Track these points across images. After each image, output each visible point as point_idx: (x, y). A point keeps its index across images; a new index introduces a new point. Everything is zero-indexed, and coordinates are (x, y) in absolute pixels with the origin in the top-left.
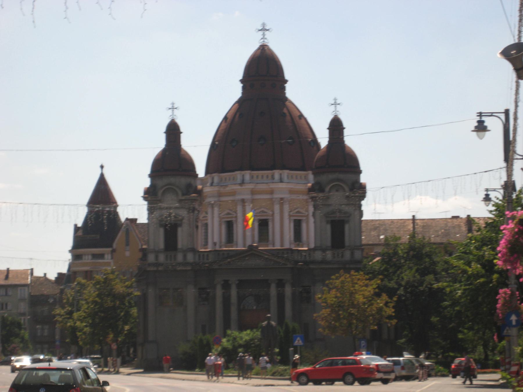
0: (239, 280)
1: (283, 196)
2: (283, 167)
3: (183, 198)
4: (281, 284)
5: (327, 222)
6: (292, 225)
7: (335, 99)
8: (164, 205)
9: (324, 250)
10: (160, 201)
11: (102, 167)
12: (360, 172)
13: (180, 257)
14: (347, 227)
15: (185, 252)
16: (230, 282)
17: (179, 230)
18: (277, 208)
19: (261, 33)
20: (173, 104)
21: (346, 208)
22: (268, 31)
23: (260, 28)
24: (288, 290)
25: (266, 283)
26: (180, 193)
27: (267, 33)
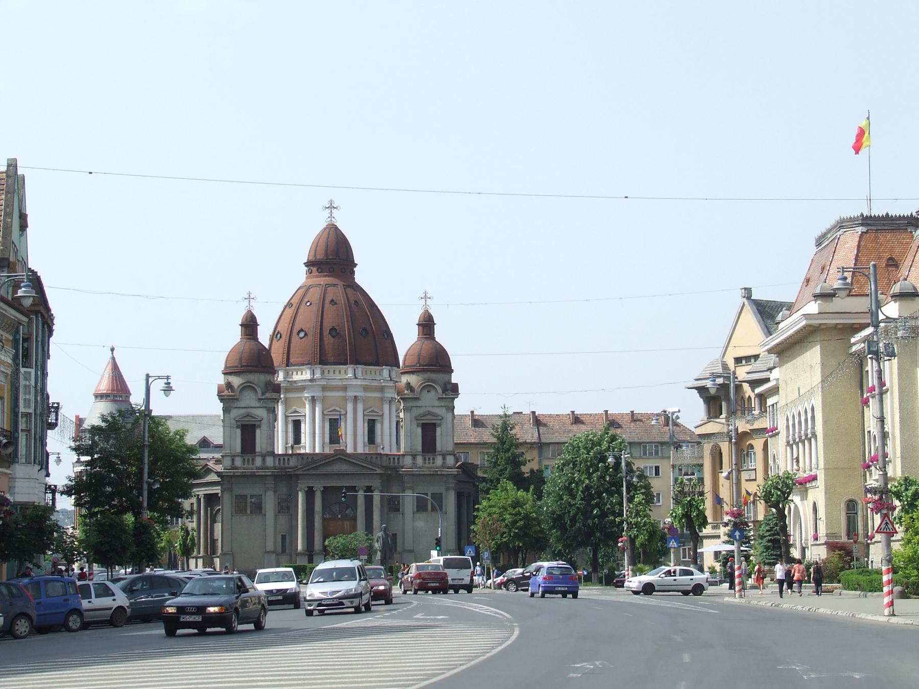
0: (323, 487)
4: (369, 489)
5: (418, 425)
6: (366, 425)
11: (112, 350)
12: (452, 371)
13: (258, 462)
14: (438, 430)
16: (314, 489)
17: (258, 432)
18: (350, 407)
19: (328, 211)
20: (249, 293)
21: (437, 411)
22: (335, 209)
23: (327, 207)
24: (377, 496)
25: (353, 489)
27: (334, 211)
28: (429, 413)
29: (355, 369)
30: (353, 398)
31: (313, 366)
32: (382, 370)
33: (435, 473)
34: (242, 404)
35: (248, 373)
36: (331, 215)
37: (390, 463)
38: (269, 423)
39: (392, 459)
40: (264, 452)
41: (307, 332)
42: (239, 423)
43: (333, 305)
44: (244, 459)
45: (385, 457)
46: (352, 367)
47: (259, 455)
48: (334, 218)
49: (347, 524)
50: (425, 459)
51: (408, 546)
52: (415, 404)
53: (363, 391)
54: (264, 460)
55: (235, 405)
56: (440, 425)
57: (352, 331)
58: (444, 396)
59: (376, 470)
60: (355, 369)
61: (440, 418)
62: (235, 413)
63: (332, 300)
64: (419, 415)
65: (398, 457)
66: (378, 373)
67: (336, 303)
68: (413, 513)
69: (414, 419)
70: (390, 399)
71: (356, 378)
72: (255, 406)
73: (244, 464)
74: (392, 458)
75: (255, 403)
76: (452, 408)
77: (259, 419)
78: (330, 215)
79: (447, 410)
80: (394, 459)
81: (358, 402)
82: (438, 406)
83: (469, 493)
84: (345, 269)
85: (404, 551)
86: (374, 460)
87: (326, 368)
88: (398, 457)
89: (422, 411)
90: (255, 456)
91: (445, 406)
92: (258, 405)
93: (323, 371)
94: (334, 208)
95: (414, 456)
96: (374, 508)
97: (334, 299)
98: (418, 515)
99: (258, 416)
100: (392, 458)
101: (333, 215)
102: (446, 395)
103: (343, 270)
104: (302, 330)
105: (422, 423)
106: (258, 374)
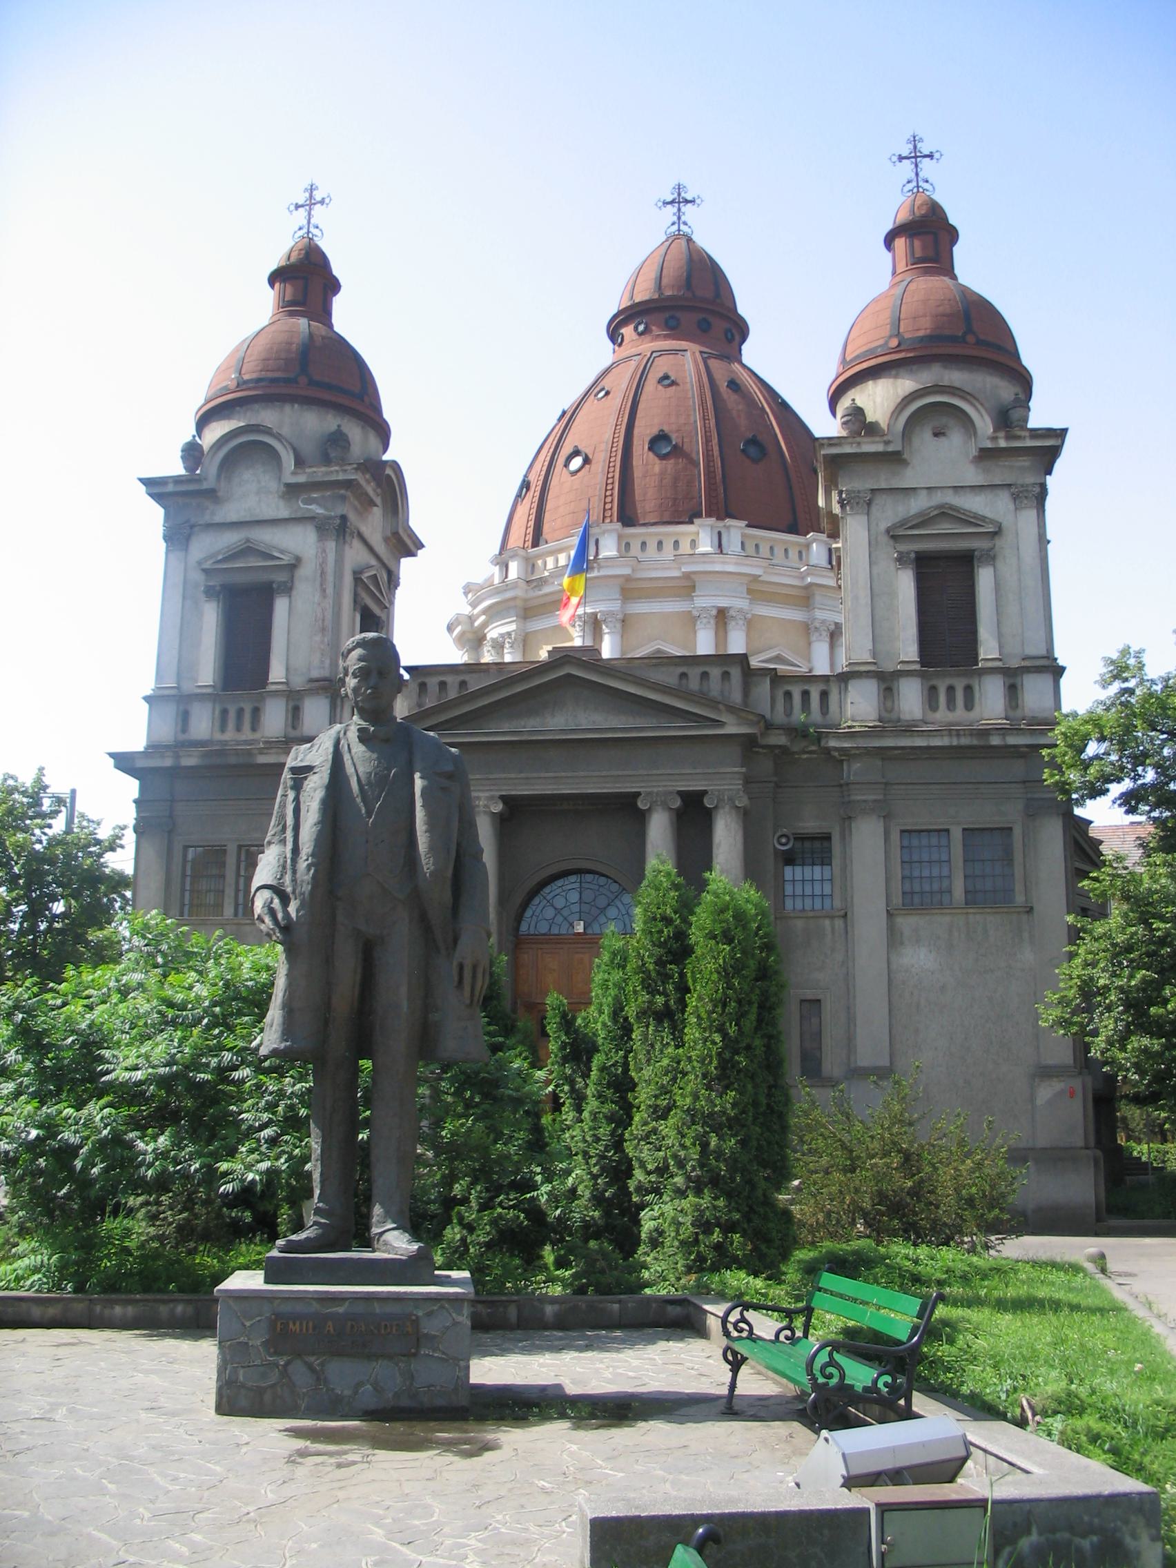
0: (502, 798)
1: (723, 603)
3: (301, 479)
5: (901, 560)
7: (914, 140)
8: (231, 511)
9: (887, 681)
10: (211, 495)
14: (984, 578)
17: (281, 606)
19: (672, 209)
21: (975, 504)
22: (689, 205)
23: (669, 199)
26: (288, 461)
27: (687, 209)
28: (946, 513)
29: (720, 534)
30: (714, 612)
32: (808, 546)
33: (975, 742)
34: (231, 511)
35: (256, 406)
36: (679, 218)
37: (789, 712)
38: (323, 573)
40: (298, 682)
41: (590, 457)
42: (215, 582)
43: (640, 334)
44: (224, 712)
45: (767, 683)
46: (712, 527)
47: (276, 693)
48: (685, 223)
50: (932, 692)
51: (869, 1053)
52: (883, 480)
53: (745, 595)
55: (207, 518)
56: (990, 557)
57: (715, 441)
58: (1003, 443)
60: (720, 534)
63: (666, 377)
64: (902, 524)
65: (822, 687)
66: (793, 554)
67: (674, 383)
68: (890, 914)
69: (884, 539)
70: (832, 627)
71: (721, 552)
73: (223, 729)
75: (276, 508)
76: (1037, 489)
77: (286, 559)
78: (675, 218)
79: (1016, 498)
80: (806, 694)
82: (981, 487)
85: (857, 1073)
86: (715, 686)
87: (634, 536)
88: (822, 687)
89: (918, 504)
90: (262, 698)
91: (1010, 485)
92: (284, 513)
93: (628, 545)
94: (687, 201)
95: (887, 681)
97: (670, 374)
98: (906, 923)
99: (282, 552)
101: (683, 218)
106: (296, 406)
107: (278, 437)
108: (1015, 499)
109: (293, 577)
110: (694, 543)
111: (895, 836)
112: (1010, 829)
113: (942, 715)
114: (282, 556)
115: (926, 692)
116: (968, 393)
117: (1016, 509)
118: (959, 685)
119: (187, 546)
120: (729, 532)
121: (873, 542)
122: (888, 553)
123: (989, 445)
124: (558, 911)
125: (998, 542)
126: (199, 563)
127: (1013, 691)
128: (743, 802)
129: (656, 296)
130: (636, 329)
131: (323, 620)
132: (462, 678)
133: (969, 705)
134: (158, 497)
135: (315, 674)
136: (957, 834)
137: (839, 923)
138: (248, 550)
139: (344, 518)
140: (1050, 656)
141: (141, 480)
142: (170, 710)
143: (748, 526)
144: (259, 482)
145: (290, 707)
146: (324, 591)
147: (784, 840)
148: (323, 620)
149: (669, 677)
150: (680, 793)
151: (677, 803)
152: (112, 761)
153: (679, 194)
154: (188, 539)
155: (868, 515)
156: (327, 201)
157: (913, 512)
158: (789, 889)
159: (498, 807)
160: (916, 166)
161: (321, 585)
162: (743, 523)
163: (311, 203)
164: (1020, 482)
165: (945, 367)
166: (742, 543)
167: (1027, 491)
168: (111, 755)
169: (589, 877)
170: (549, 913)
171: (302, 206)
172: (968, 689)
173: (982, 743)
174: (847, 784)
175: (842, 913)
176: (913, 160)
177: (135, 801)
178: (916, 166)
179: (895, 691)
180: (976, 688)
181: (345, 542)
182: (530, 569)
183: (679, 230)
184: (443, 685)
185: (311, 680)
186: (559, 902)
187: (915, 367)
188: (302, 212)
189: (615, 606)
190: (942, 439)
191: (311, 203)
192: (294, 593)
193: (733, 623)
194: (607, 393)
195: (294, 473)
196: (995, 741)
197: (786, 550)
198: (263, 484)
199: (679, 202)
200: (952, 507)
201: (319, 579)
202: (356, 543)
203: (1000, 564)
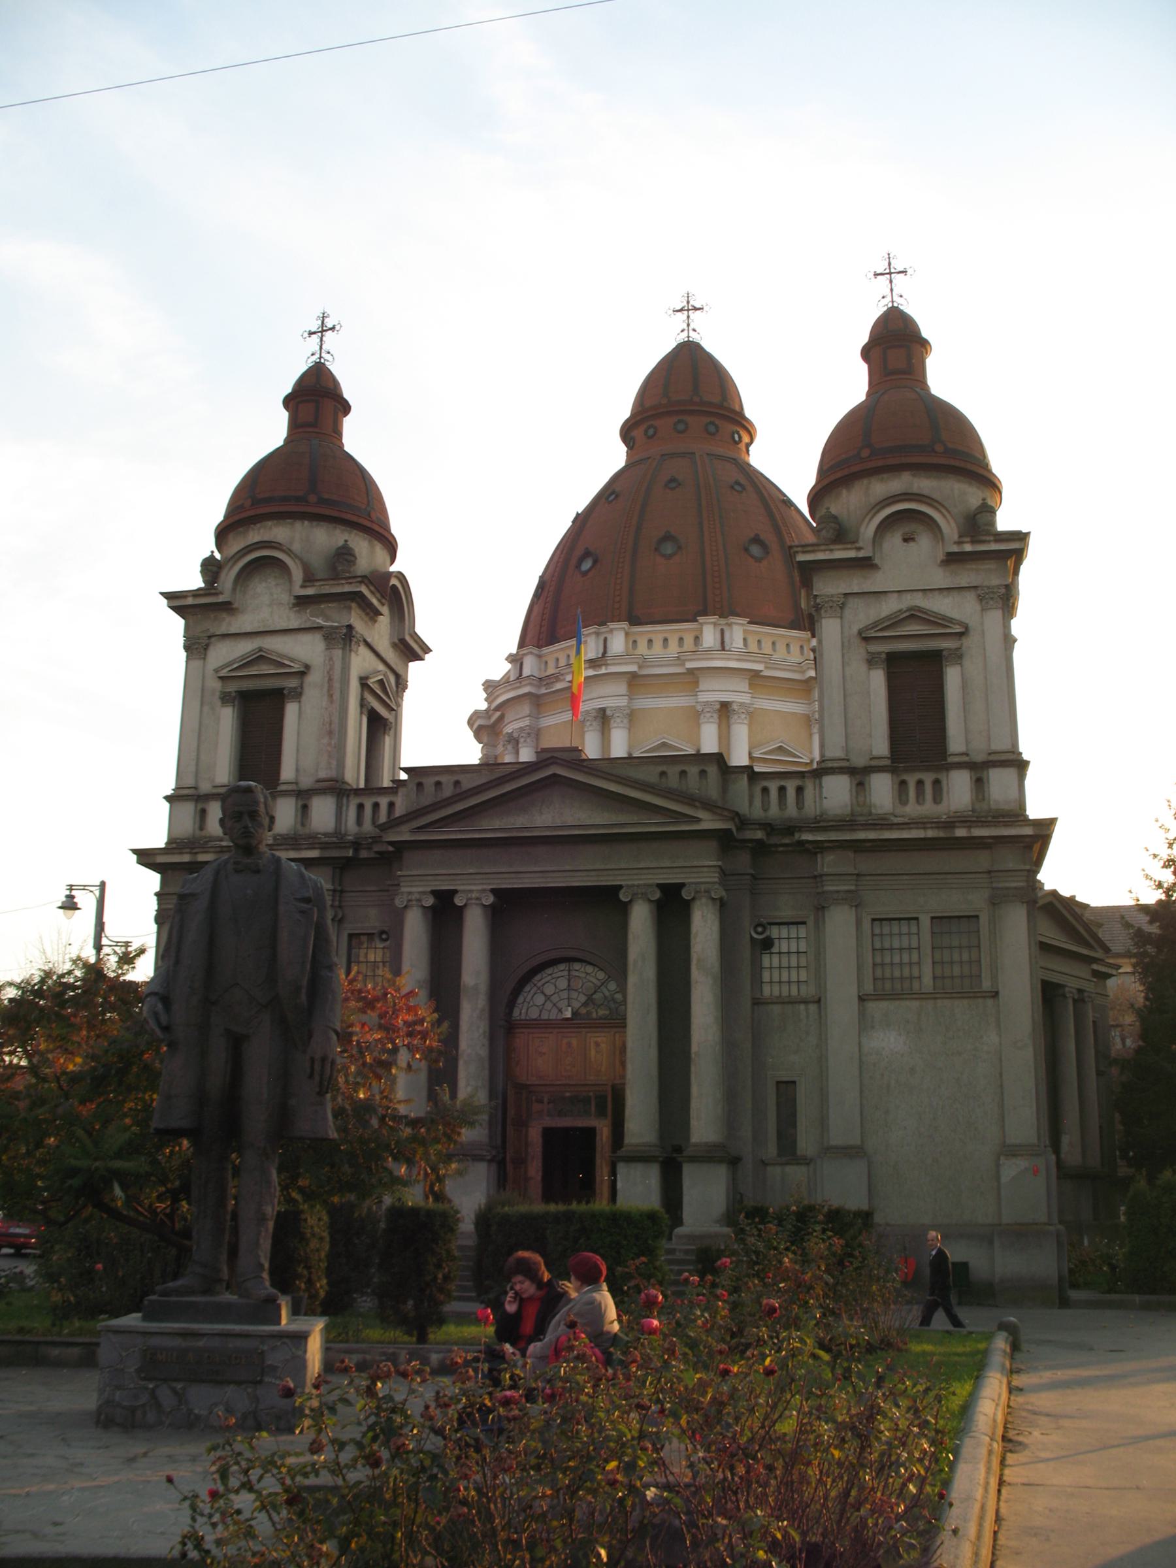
0: (493, 891)
2: (726, 610)
3: (310, 591)
5: (871, 661)
9: (859, 774)
10: (227, 607)
14: (952, 676)
15: (303, 796)
17: (291, 709)
21: (942, 605)
26: (297, 574)
28: (914, 615)
29: (722, 631)
30: (718, 706)
31: (603, 629)
33: (941, 834)
35: (270, 523)
36: (688, 325)
37: (766, 807)
38: (330, 680)
39: (774, 794)
40: (306, 782)
42: (232, 687)
45: (744, 779)
46: (715, 624)
47: (286, 793)
48: (694, 330)
49: (597, 1044)
51: (841, 1132)
52: (856, 583)
53: (747, 689)
54: (304, 810)
55: (223, 629)
56: (957, 656)
58: (968, 548)
59: (698, 820)
60: (722, 631)
61: (958, 629)
62: (223, 654)
63: (673, 480)
64: (875, 625)
65: (797, 782)
68: (862, 999)
71: (723, 649)
72: (283, 625)
74: (773, 787)
77: (297, 667)
78: (685, 326)
79: (981, 599)
80: (782, 790)
81: (732, 721)
83: (1080, 991)
84: (717, 427)
85: (830, 1151)
86: (693, 784)
89: (889, 607)
92: (295, 623)
93: (635, 642)
95: (859, 774)
96: (695, 974)
99: (292, 660)
100: (773, 787)
101: (692, 326)
102: (973, 542)
103: (712, 429)
104: (587, 554)
105: (888, 654)
106: (306, 523)
107: (289, 552)
108: (981, 600)
109: (302, 684)
110: (697, 639)
111: (866, 925)
112: (977, 917)
113: (912, 809)
114: (292, 664)
115: (896, 786)
116: (937, 502)
117: (983, 610)
118: (928, 778)
119: (205, 655)
120: (732, 630)
121: (846, 644)
122: (859, 652)
123: (955, 549)
124: (548, 998)
125: (966, 642)
126: (216, 671)
127: (979, 783)
128: (721, 893)
129: (664, 401)
130: (646, 431)
131: (330, 724)
132: (456, 778)
133: (937, 798)
134: (178, 610)
135: (322, 774)
136: (925, 921)
137: (813, 1008)
138: (261, 657)
139: (350, 627)
140: (1014, 750)
141: (162, 594)
142: (189, 808)
143: (749, 623)
144: (271, 594)
145: (299, 806)
146: (331, 696)
147: (760, 929)
148: (330, 724)
149: (650, 775)
150: (659, 886)
151: (657, 895)
152: (135, 857)
153: (688, 302)
154: (206, 647)
155: (841, 618)
156: (337, 328)
157: (883, 615)
158: (766, 976)
159: (489, 900)
160: (891, 282)
161: (328, 691)
162: (744, 621)
163: (323, 331)
164: (986, 583)
165: (914, 476)
166: (745, 639)
167: (993, 592)
168: (135, 851)
169: (577, 966)
170: (540, 999)
171: (314, 333)
172: (937, 783)
173: (949, 835)
174: (821, 876)
175: (816, 998)
176: (888, 276)
177: (157, 894)
178: (891, 282)
179: (867, 786)
180: (944, 782)
181: (350, 650)
182: (543, 666)
183: (688, 337)
184: (438, 784)
185: (318, 781)
186: (549, 990)
187: (885, 476)
188: (316, 338)
189: (623, 702)
190: (912, 544)
191: (323, 331)
192: (304, 698)
193: (736, 717)
194: (617, 496)
195: (303, 587)
196: (961, 832)
197: (788, 645)
198: (275, 596)
199: (688, 310)
200: (920, 609)
201: (326, 685)
202: (363, 650)
203: (966, 662)
